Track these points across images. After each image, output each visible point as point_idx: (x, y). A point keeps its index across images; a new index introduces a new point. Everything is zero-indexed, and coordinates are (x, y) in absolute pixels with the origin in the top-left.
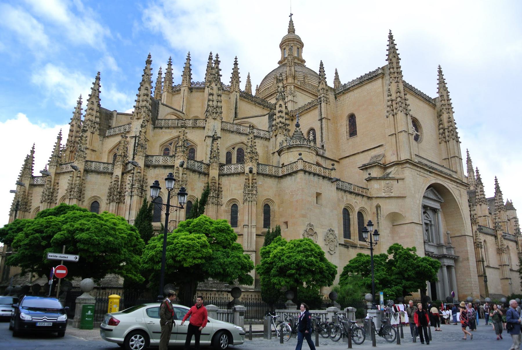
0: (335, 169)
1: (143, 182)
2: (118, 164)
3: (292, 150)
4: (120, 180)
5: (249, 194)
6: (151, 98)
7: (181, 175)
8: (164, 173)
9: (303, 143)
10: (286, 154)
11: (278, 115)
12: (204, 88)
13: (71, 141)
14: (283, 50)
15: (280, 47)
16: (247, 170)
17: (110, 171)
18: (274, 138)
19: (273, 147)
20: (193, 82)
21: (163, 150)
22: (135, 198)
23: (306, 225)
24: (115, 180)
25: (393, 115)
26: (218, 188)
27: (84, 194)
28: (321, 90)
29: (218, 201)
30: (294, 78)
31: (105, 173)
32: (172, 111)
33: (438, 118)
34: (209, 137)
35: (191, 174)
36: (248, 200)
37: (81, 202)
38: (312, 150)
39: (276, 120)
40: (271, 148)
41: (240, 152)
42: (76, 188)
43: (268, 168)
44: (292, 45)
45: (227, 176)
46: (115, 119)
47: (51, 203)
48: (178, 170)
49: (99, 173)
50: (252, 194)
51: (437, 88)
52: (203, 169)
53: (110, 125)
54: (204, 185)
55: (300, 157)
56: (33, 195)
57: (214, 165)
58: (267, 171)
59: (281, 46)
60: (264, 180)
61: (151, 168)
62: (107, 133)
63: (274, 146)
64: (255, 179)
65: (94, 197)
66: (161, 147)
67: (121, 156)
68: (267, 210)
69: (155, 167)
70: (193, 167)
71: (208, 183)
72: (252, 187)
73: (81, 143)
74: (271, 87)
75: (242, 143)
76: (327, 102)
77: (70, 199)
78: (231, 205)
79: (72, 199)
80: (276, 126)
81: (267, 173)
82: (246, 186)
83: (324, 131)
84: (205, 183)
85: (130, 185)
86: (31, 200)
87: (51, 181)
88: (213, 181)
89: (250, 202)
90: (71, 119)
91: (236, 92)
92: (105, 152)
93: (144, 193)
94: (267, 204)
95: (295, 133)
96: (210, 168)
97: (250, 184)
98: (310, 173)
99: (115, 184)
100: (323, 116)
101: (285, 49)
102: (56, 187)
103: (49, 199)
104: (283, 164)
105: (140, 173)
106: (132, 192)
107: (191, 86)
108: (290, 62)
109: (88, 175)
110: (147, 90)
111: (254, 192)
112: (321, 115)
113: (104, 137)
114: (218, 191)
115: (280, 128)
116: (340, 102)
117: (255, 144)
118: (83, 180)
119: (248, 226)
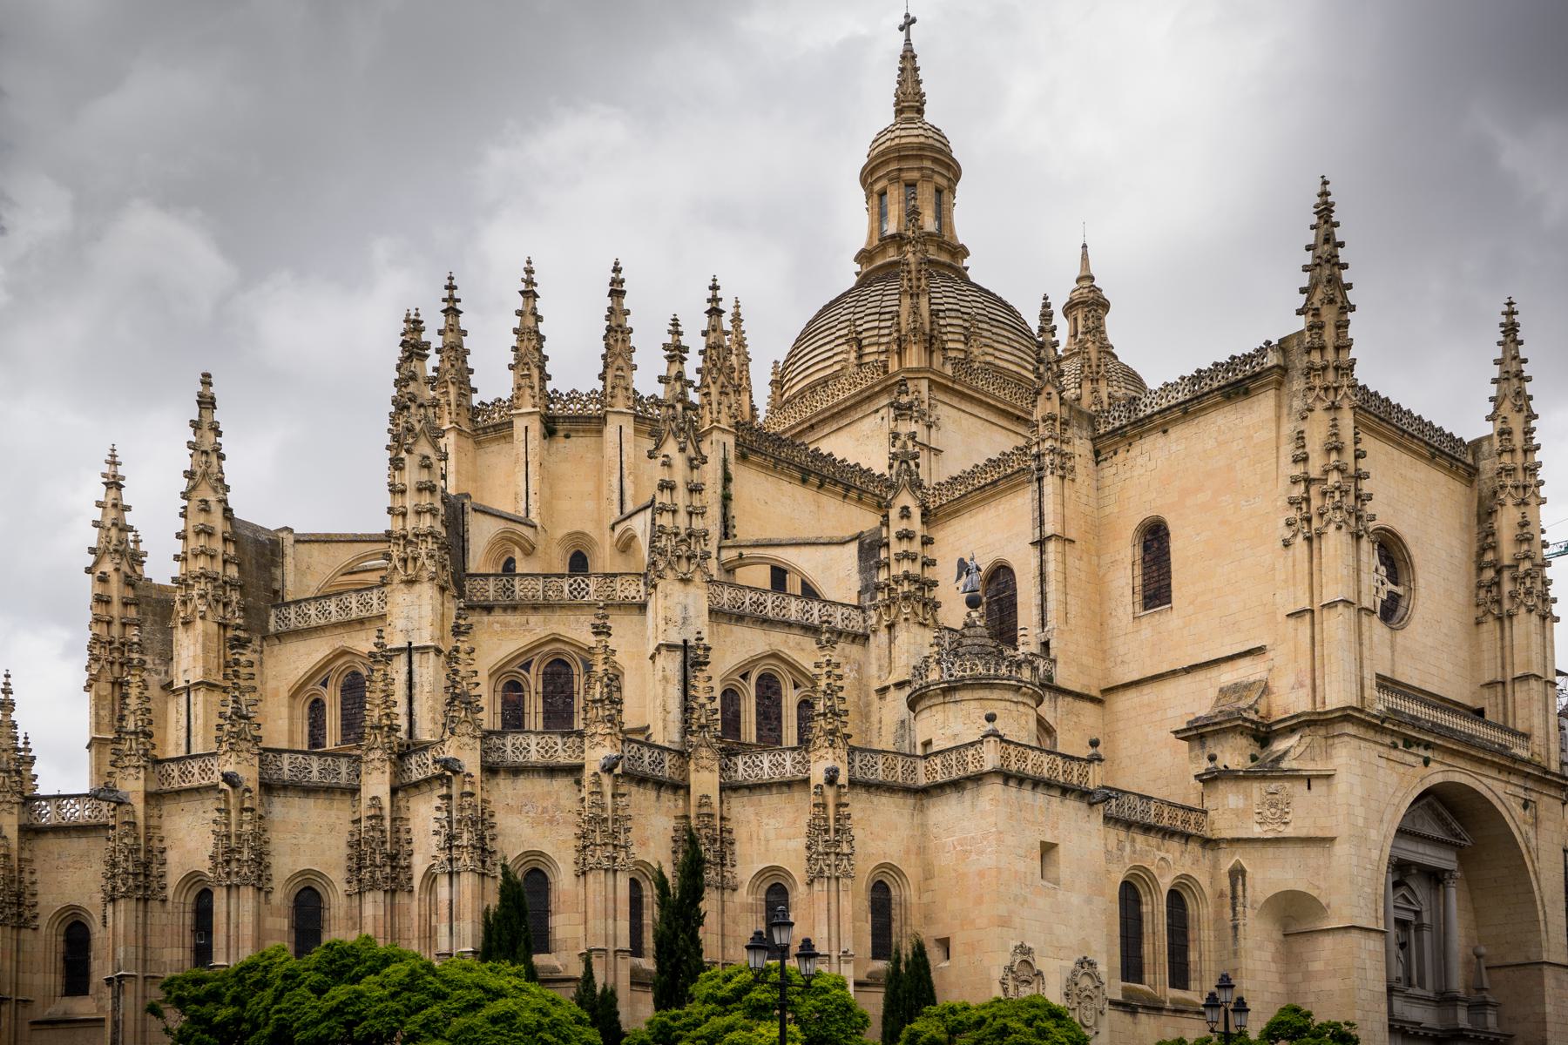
0: (1100, 760)
1: (483, 824)
2: (371, 756)
3: (958, 696)
4: (387, 812)
5: (827, 854)
6: (445, 499)
7: (608, 800)
8: (549, 793)
9: (996, 671)
10: (939, 708)
11: (897, 547)
12: (602, 420)
13: (111, 643)
14: (876, 197)
15: (864, 181)
16: (818, 774)
17: (343, 780)
18: (883, 635)
19: (880, 667)
20: (555, 391)
21: (500, 688)
22: (467, 882)
23: (1012, 949)
24: (372, 812)
25: (1309, 540)
26: (721, 831)
27: (268, 867)
28: (1041, 425)
29: (723, 877)
30: (931, 342)
31: (328, 791)
32: (500, 525)
33: (1480, 522)
34: (670, 647)
35: (634, 789)
36: (826, 874)
37: (262, 894)
38: (1025, 694)
39: (888, 565)
40: (873, 670)
41: (769, 688)
42: (246, 851)
43: (880, 763)
44: (915, 175)
45: (746, 792)
46: (289, 561)
47: (146, 900)
48: (598, 783)
49: (309, 790)
50: (837, 854)
51: (1492, 399)
52: (668, 769)
53: (277, 586)
54: (673, 823)
55: (989, 726)
56: (36, 866)
57: (704, 754)
58: (880, 771)
59: (868, 176)
60: (872, 802)
61: (502, 775)
62: (272, 620)
63: (885, 662)
64: (846, 805)
65: (302, 873)
66: (493, 681)
67: (381, 728)
68: (881, 900)
69: (517, 771)
70: (636, 764)
71: (687, 817)
72: (837, 831)
73: (237, 687)
74: (836, 376)
75: (775, 655)
76: (1065, 472)
77: (229, 887)
78: (766, 886)
79: (238, 887)
80: (891, 590)
81: (881, 776)
82: (816, 829)
83: (1051, 588)
84: (676, 817)
85: (443, 838)
86: (33, 883)
87: (134, 824)
88: (705, 810)
89: (833, 882)
90: (92, 551)
91: (723, 430)
92: (276, 693)
93: (488, 860)
94: (881, 882)
95: (966, 631)
96: (692, 766)
97: (832, 822)
98: (1021, 779)
99: (373, 828)
100: (1049, 529)
101: (882, 194)
102: (156, 844)
103: (138, 887)
104: (927, 744)
105: (472, 795)
106: (450, 860)
107: (549, 409)
108: (914, 274)
109: (276, 800)
110: (429, 467)
111: (845, 849)
112: (1042, 523)
113: (264, 638)
114: (722, 842)
115: (906, 597)
116: (1113, 470)
117: (839, 683)
118: (261, 817)
119: (829, 956)
